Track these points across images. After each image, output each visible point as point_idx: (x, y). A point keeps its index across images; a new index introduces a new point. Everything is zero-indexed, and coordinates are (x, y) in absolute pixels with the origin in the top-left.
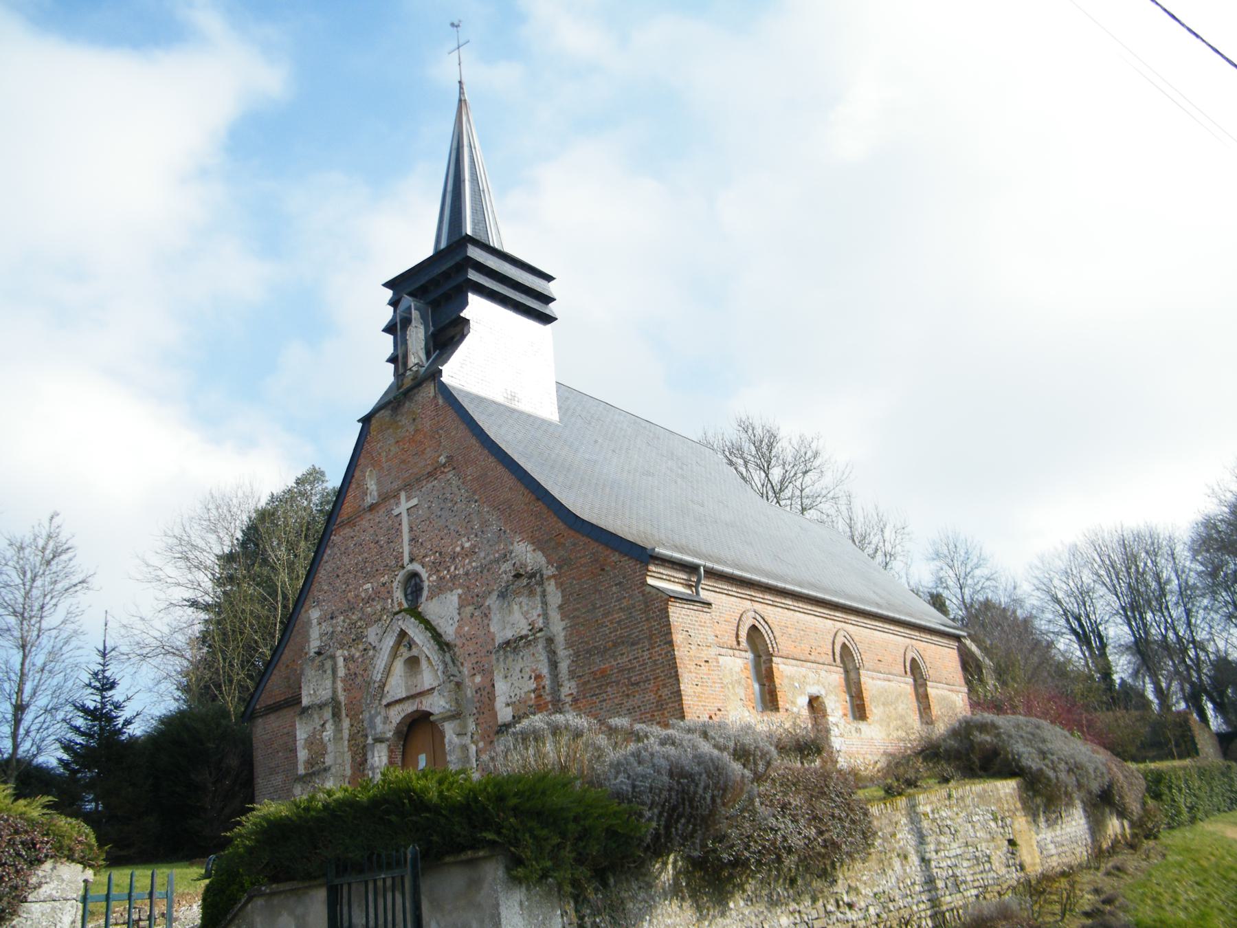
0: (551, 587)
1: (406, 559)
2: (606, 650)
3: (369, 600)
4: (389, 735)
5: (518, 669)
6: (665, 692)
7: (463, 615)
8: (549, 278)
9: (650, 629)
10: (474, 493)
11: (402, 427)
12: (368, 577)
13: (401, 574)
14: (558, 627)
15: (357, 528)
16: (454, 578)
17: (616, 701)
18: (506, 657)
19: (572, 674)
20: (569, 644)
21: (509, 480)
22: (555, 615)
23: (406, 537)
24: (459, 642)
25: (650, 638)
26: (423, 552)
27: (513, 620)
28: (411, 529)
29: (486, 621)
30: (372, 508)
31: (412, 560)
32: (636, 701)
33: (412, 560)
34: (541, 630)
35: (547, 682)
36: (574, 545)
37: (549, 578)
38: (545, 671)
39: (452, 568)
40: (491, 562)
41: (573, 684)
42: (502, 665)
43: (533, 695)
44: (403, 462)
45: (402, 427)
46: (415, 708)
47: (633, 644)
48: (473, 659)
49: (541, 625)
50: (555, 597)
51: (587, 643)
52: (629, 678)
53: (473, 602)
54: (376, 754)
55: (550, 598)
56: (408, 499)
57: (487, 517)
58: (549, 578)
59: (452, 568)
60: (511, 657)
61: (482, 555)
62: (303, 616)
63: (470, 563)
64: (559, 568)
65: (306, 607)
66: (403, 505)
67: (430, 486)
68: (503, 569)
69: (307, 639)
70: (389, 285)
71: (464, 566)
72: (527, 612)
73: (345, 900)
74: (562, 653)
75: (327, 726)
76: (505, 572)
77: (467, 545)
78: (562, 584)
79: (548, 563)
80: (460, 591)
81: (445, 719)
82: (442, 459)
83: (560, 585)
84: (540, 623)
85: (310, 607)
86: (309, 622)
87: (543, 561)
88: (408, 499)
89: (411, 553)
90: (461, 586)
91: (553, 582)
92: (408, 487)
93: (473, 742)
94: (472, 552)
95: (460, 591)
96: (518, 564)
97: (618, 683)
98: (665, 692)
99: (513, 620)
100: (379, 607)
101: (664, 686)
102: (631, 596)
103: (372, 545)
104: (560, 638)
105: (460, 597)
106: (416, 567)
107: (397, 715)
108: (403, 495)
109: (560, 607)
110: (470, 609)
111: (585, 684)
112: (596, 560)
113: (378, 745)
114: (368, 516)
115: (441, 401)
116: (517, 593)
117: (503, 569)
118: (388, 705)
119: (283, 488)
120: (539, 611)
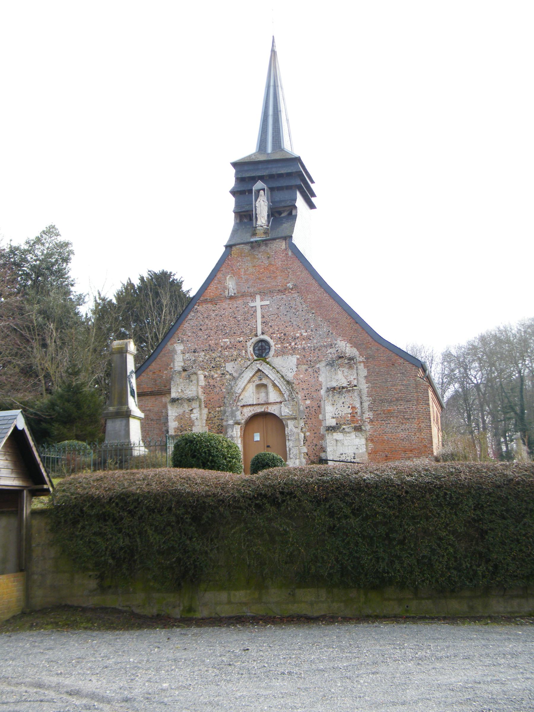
0: (361, 366)
1: (259, 332)
2: (391, 401)
3: (227, 348)
4: (243, 421)
5: (341, 402)
6: (423, 425)
7: (300, 369)
8: (313, 182)
9: (418, 396)
10: (312, 308)
11: (259, 259)
12: (226, 335)
13: (254, 340)
14: (364, 386)
15: (217, 306)
16: (294, 349)
17: (395, 425)
18: (334, 395)
19: (371, 409)
20: (370, 395)
21: (337, 308)
22: (363, 381)
23: (259, 320)
24: (295, 381)
25: (417, 400)
26: (271, 330)
27: (341, 378)
28: (263, 317)
29: (316, 375)
30: (231, 298)
31: (263, 333)
32: (407, 426)
33: (263, 333)
34: (355, 386)
35: (359, 411)
36: (378, 350)
37: (360, 362)
38: (358, 405)
39: (293, 344)
40: (321, 346)
41: (371, 414)
42: (331, 398)
43: (349, 415)
44: (259, 279)
45: (259, 259)
46: (263, 410)
47: (407, 401)
48: (306, 392)
49: (355, 384)
50: (363, 372)
51: (381, 396)
52: (404, 416)
53: (308, 362)
54: (234, 430)
55: (360, 372)
56: (262, 300)
57: (320, 323)
58: (360, 362)
59: (293, 344)
60: (337, 396)
61: (315, 341)
62: (169, 346)
63: (305, 343)
64: (367, 359)
65: (173, 340)
66: (258, 303)
67: (279, 297)
68: (329, 351)
69: (173, 360)
70: (235, 165)
71: (301, 344)
72: (347, 376)
73: (10, 509)
74: (365, 398)
75: (194, 411)
76: (331, 353)
77: (305, 334)
78: (368, 367)
79: (360, 355)
80: (298, 356)
81: (288, 419)
82: (290, 285)
83: (365, 367)
84: (355, 382)
85: (175, 343)
86: (174, 351)
87: (357, 353)
88: (262, 300)
89: (262, 329)
90: (299, 354)
91: (362, 364)
92: (263, 294)
93: (302, 432)
94: (308, 338)
95: (298, 356)
96: (339, 351)
97: (397, 417)
98: (423, 425)
99: (341, 378)
100: (235, 353)
101: (423, 422)
102: (408, 380)
103: (231, 319)
104: (365, 391)
105: (298, 359)
106: (266, 337)
107: (248, 412)
108: (258, 297)
109: (366, 377)
110: (304, 367)
111: (378, 414)
112: (390, 360)
113: (237, 426)
114: (228, 301)
115: (290, 253)
116: (340, 366)
117: (329, 351)
118: (244, 406)
119: (464, 343)
120: (355, 376)
